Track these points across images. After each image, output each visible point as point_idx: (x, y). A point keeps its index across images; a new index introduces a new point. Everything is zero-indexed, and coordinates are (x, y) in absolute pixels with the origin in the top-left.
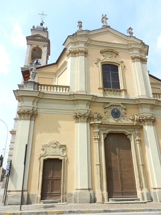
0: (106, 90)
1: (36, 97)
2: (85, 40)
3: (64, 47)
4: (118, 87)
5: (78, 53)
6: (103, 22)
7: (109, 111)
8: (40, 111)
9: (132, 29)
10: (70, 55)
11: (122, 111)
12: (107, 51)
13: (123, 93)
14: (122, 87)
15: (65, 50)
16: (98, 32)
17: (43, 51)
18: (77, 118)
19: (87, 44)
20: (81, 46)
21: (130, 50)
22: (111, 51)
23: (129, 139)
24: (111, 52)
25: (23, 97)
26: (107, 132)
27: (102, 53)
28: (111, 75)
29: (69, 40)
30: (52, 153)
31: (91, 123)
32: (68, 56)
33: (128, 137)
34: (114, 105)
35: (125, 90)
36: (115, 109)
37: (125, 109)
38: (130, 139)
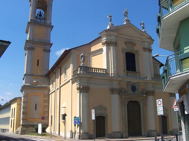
0: (128, 72)
1: (89, 78)
2: (116, 34)
3: (99, 36)
4: (135, 71)
6: (125, 15)
7: (130, 87)
8: (91, 86)
9: (144, 24)
11: (137, 87)
12: (129, 43)
13: (138, 74)
15: (100, 38)
16: (123, 27)
17: (48, 4)
18: (113, 91)
19: (116, 37)
20: (113, 39)
23: (139, 104)
24: (132, 43)
26: (129, 101)
27: (126, 44)
28: (130, 61)
29: (105, 33)
30: (102, 113)
31: (121, 95)
32: (103, 44)
33: (139, 103)
35: (139, 73)
36: (134, 86)
37: (139, 86)
38: (140, 105)
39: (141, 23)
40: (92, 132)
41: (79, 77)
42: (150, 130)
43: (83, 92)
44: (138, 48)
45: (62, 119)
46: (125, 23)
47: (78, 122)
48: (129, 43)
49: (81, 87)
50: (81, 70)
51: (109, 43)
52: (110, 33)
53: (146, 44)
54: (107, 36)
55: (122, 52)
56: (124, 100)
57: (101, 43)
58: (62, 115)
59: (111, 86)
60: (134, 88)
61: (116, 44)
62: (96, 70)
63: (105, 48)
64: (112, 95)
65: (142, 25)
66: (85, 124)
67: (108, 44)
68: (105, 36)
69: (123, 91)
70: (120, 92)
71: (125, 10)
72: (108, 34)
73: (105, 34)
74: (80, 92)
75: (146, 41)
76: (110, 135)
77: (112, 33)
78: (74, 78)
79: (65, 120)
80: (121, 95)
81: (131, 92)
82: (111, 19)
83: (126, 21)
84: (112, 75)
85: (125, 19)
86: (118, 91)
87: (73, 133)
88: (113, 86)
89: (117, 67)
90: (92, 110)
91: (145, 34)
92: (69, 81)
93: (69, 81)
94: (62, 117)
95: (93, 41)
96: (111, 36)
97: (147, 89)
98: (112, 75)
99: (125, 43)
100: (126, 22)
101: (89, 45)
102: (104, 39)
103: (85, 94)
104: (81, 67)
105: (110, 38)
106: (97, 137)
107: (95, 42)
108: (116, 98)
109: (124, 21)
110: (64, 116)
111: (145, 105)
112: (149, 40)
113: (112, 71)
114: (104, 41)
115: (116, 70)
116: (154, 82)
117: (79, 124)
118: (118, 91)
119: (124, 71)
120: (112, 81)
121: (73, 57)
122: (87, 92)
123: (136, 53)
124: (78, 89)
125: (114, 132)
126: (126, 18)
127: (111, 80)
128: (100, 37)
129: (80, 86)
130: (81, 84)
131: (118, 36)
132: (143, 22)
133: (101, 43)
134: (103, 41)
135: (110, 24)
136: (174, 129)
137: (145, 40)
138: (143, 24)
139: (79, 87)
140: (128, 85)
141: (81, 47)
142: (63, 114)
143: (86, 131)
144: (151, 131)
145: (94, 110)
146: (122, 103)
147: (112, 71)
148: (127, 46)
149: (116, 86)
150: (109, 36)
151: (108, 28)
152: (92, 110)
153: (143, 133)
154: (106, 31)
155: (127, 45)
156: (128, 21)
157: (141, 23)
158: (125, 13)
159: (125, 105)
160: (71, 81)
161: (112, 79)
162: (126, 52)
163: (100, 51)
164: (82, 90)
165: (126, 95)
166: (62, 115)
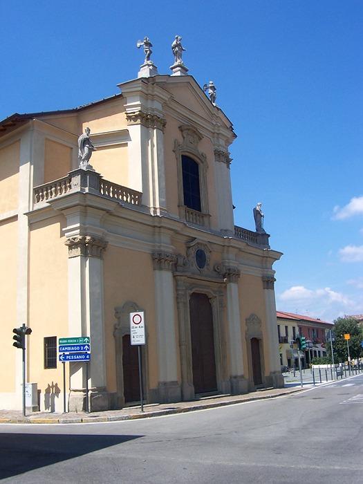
1: (108, 211)
2: (165, 96)
5: (153, 121)
6: (175, 54)
7: (193, 252)
8: (111, 240)
10: (139, 121)
11: (207, 254)
12: (189, 130)
13: (206, 219)
14: (204, 211)
18: (158, 259)
19: (165, 104)
21: (216, 134)
22: (190, 130)
25: (88, 208)
26: (194, 290)
27: (182, 131)
28: (190, 180)
31: (178, 273)
32: (129, 118)
34: (198, 243)
36: (202, 251)
39: (206, 85)
40: (116, 388)
41: (81, 203)
42: (234, 374)
43: (93, 256)
44: (205, 149)
45: (15, 345)
46: (179, 74)
47: (70, 355)
48: (189, 130)
49: (88, 238)
50: (83, 184)
51: (148, 119)
52: (153, 92)
53: (222, 142)
54: (146, 96)
55: (174, 151)
56: (184, 288)
57: (123, 116)
58: (15, 331)
59: (154, 246)
60: (201, 258)
61: (164, 126)
62: (118, 190)
63: (135, 131)
64: (157, 272)
65: (210, 91)
66: (99, 362)
67: (147, 120)
68: (139, 97)
69: (181, 261)
70: (176, 266)
71: (177, 38)
72: (147, 90)
73: (140, 89)
74: (84, 255)
75: (223, 133)
76: (156, 392)
77: (157, 91)
78: (55, 209)
79: (24, 349)
80: (178, 273)
81: (194, 267)
82: (151, 52)
83: (178, 68)
84: (155, 212)
85: (176, 64)
86: (171, 263)
87: (39, 392)
88: (159, 247)
89: (165, 192)
90: (132, 315)
91: (220, 115)
92: (15, 218)
93: (15, 218)
94: (15, 338)
95: (105, 101)
96: (153, 100)
97: (227, 264)
98: (155, 212)
99: (179, 127)
100: (179, 70)
101: (75, 114)
102: (134, 106)
103: (98, 262)
104: (83, 174)
105: (149, 104)
106: (126, 401)
107: (102, 108)
108: (166, 278)
109: (172, 69)
110: (20, 336)
111: (223, 306)
112: (229, 134)
113: (155, 202)
114: (137, 110)
115: (164, 200)
116: (241, 245)
117: (85, 358)
118: (171, 263)
119: (179, 206)
120: (157, 229)
121: (28, 142)
122: (101, 257)
123: (202, 162)
124: (72, 245)
125: (165, 384)
126: (179, 61)
127: (156, 226)
128: (121, 96)
129: (84, 234)
130: (86, 229)
131: (168, 102)
132: (211, 82)
133: (123, 116)
134: (129, 110)
135: (149, 65)
136: (274, 373)
137: (221, 132)
138: (213, 88)
139: (80, 237)
140: (189, 248)
141: (58, 116)
142: (18, 327)
143: (102, 384)
144: (235, 377)
145: (142, 314)
146: (177, 298)
147: (155, 202)
148: (184, 138)
149: (166, 245)
150: (147, 99)
151: (144, 73)
152: (132, 315)
153: (222, 383)
154: (144, 80)
155: (185, 136)
156: (184, 69)
157: (206, 85)
158: (176, 46)
159: (185, 303)
160: (23, 221)
161: (159, 225)
162: (184, 154)
163: (120, 138)
164: (90, 248)
165: (189, 274)
166: (15, 331)
